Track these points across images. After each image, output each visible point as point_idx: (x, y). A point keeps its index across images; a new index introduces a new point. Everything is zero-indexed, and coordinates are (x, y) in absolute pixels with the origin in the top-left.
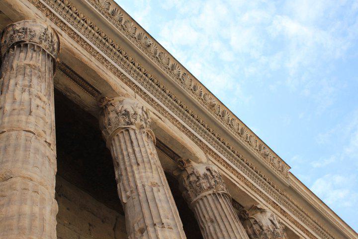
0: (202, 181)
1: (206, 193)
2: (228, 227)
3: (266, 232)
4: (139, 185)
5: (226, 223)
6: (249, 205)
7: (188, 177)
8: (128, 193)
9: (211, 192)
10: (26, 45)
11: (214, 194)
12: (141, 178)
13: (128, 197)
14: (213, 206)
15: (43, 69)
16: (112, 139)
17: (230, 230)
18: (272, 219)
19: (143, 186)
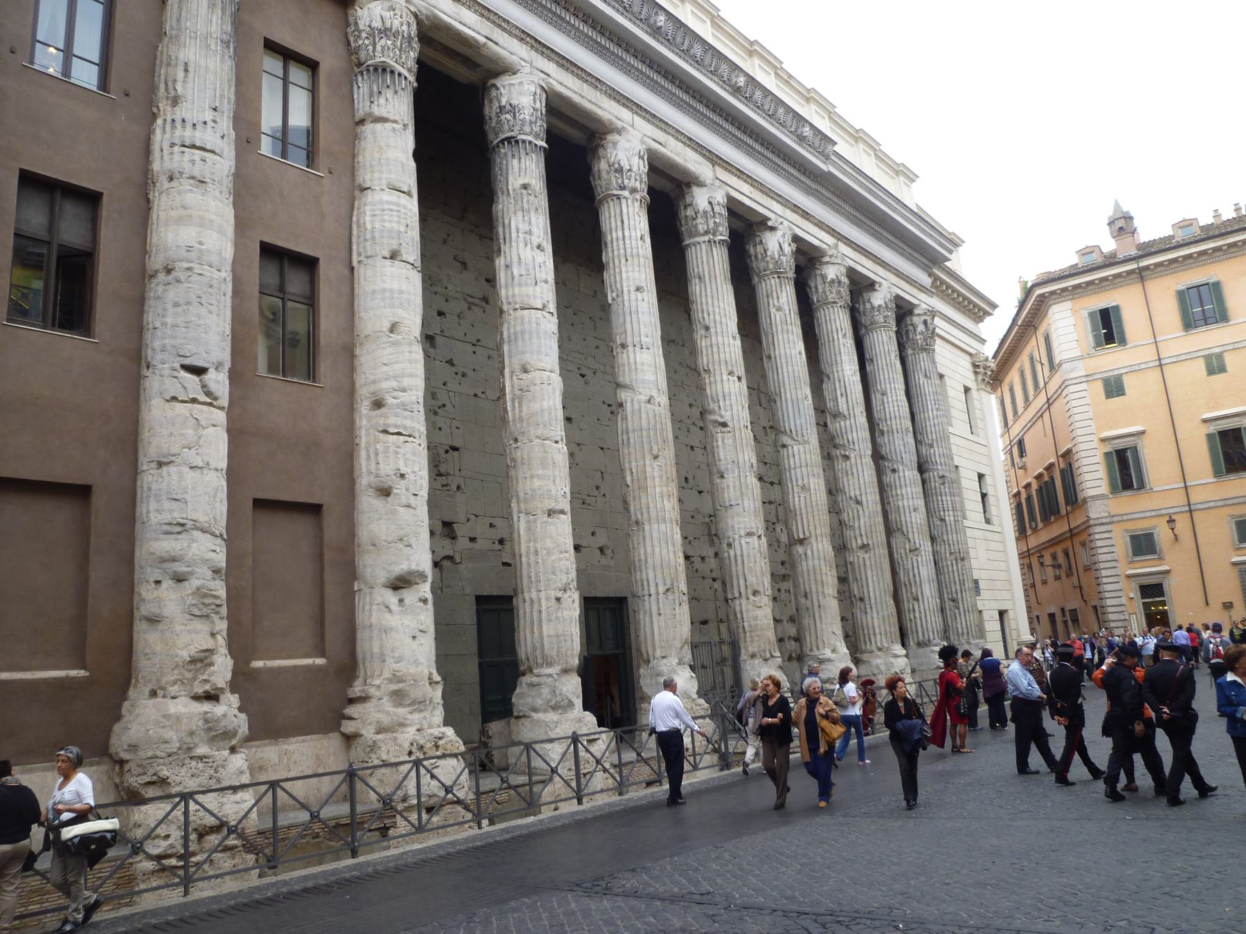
0: (699, 220)
1: (700, 239)
2: (715, 291)
3: (768, 259)
4: (625, 289)
5: (714, 287)
6: (759, 219)
7: (685, 208)
8: (614, 295)
9: (706, 238)
10: (517, 142)
11: (709, 241)
12: (628, 278)
13: (613, 299)
14: (705, 259)
15: (537, 188)
16: (601, 202)
17: (716, 296)
18: (781, 241)
19: (629, 291)
